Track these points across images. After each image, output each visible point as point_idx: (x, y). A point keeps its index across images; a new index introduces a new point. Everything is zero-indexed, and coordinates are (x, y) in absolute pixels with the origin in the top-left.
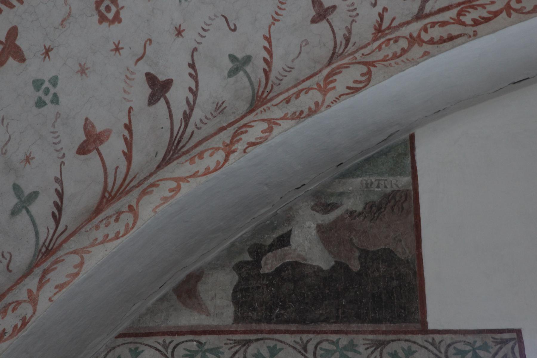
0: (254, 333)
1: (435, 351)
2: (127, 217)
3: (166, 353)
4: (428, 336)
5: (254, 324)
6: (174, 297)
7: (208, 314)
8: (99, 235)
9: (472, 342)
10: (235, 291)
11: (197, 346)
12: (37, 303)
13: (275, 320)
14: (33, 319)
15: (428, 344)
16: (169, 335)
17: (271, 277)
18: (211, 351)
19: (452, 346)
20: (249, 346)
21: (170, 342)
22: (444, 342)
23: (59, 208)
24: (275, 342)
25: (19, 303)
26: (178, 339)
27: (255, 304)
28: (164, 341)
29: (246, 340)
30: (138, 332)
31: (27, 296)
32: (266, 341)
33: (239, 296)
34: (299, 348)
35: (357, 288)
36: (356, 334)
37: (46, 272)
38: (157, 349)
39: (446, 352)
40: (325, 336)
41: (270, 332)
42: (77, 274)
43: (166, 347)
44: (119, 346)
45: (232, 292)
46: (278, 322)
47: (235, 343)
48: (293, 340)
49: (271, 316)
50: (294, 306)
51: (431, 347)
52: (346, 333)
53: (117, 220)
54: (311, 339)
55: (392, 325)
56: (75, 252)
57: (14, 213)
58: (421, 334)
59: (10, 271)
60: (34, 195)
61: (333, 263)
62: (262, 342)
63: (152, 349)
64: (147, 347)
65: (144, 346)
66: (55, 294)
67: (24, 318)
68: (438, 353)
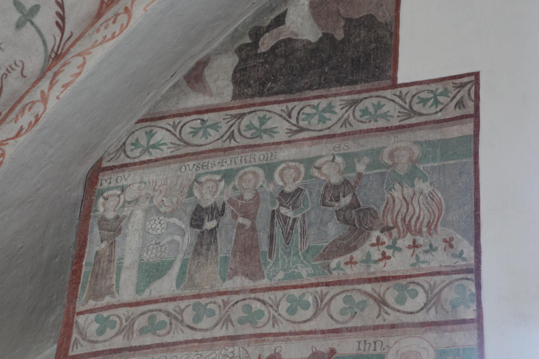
0: (248, 107)
1: (401, 102)
2: (122, 18)
3: (175, 133)
4: (396, 90)
5: (248, 99)
6: (185, 83)
7: (211, 95)
8: (99, 37)
9: (434, 89)
10: (235, 72)
11: (201, 123)
12: (47, 101)
13: (266, 93)
14: (44, 115)
15: (395, 97)
16: (178, 117)
17: (266, 55)
18: (211, 126)
19: (417, 96)
20: (243, 118)
21: (179, 123)
22: (410, 93)
23: (62, 18)
24: (264, 113)
25: (33, 103)
26: (185, 119)
27: (250, 81)
28: (174, 122)
29: (241, 114)
30: (153, 117)
31: (40, 97)
32: (258, 113)
33: (238, 75)
34: (284, 116)
35: (340, 55)
36: (335, 96)
37: (56, 74)
38: (168, 130)
39: (411, 102)
40: (307, 102)
41: (262, 104)
42: (80, 73)
43: (175, 127)
44: (137, 130)
45: (232, 73)
46: (269, 95)
47: (232, 117)
48: (280, 108)
49: (263, 90)
50: (284, 79)
51: (397, 100)
52: (326, 97)
53: (114, 22)
54: (295, 106)
55: (366, 84)
56: (79, 55)
57: (19, 26)
58: (390, 89)
59: (25, 77)
60: (36, 9)
61: (320, 35)
62: (254, 114)
63: (163, 130)
64: (160, 129)
65: (157, 128)
66: (62, 92)
67: (37, 115)
68: (403, 104)
